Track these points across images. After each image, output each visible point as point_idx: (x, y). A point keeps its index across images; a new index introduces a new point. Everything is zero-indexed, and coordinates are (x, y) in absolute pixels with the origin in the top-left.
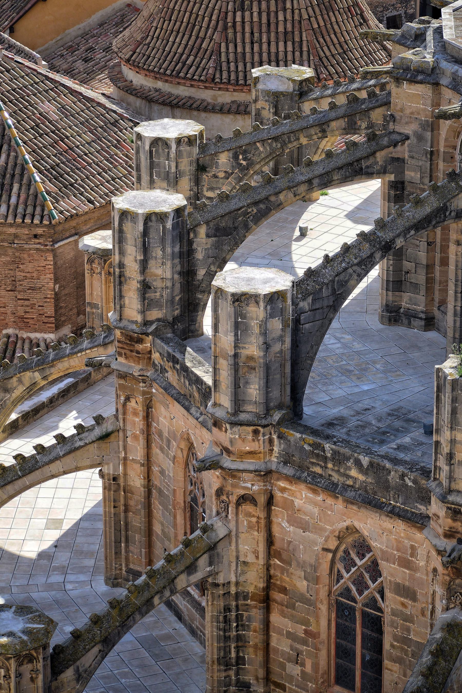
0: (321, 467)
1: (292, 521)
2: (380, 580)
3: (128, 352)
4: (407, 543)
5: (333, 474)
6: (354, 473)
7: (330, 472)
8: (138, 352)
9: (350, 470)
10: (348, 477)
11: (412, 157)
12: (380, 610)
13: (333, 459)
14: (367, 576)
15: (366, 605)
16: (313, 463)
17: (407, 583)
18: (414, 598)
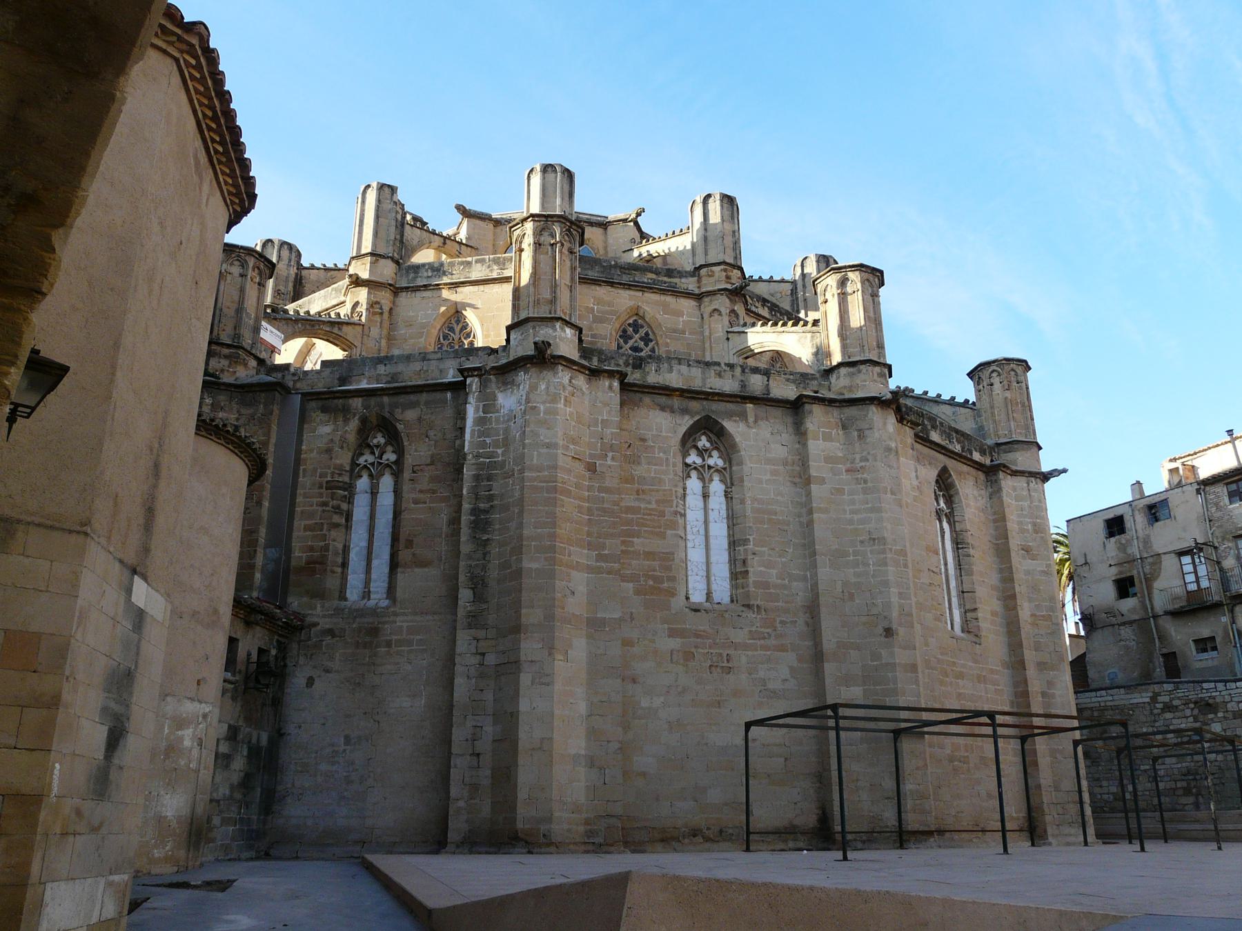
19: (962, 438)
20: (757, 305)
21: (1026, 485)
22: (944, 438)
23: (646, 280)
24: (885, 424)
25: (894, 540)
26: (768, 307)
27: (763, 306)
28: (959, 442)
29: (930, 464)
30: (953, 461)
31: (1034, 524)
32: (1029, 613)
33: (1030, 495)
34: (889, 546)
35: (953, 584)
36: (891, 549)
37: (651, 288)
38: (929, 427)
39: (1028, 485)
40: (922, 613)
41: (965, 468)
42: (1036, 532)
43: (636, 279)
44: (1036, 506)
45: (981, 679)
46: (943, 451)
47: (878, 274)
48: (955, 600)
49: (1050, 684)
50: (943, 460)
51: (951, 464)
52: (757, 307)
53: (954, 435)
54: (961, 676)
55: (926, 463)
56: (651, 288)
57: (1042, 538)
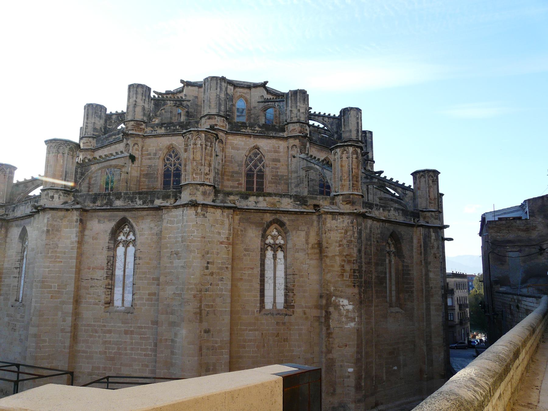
0: (245, 129)
1: (233, 148)
2: (262, 163)
3: (136, 129)
4: (277, 145)
5: (250, 130)
6: (257, 129)
7: (248, 130)
8: (141, 128)
9: (256, 128)
10: (255, 130)
11: (192, 106)
12: (263, 172)
13: (249, 126)
14: (258, 162)
15: (258, 172)
16: (242, 129)
17: (277, 158)
18: (279, 161)
19: (145, 196)
20: (156, 129)
21: (182, 213)
22: (127, 200)
23: (112, 140)
24: (44, 219)
25: (38, 276)
26: (165, 127)
27: (161, 128)
28: (140, 199)
29: (109, 220)
30: (134, 212)
31: (182, 237)
32: (173, 292)
33: (183, 218)
34: (35, 279)
35: (129, 281)
36: (35, 281)
37: (112, 144)
38: (114, 199)
39: (183, 211)
40: (64, 306)
41: (145, 213)
42: (182, 242)
43: (110, 141)
44: (185, 225)
45: (126, 332)
46: (121, 210)
47: (54, 141)
48: (129, 289)
49: (176, 335)
50: (121, 214)
51: (127, 215)
52: (156, 131)
53: (137, 196)
54: (110, 332)
55: (106, 221)
56: (112, 144)
57: (184, 245)
